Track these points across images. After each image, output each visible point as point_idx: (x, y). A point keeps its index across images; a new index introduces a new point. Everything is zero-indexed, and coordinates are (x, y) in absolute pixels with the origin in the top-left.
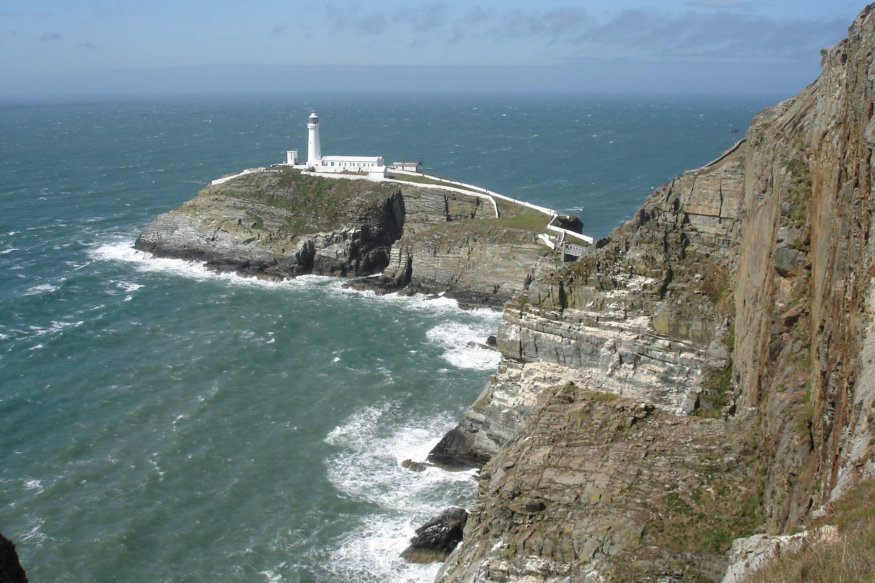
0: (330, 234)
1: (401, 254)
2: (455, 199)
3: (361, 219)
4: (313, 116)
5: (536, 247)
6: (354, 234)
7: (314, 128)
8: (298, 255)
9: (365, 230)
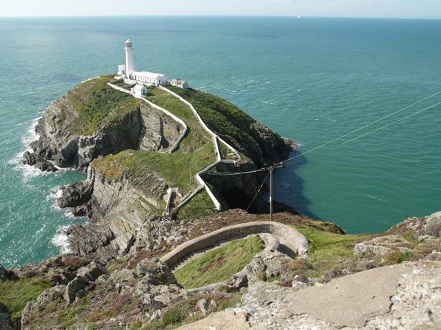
0: (84, 138)
1: (91, 171)
2: (166, 123)
4: (127, 42)
5: (155, 204)
8: (63, 151)
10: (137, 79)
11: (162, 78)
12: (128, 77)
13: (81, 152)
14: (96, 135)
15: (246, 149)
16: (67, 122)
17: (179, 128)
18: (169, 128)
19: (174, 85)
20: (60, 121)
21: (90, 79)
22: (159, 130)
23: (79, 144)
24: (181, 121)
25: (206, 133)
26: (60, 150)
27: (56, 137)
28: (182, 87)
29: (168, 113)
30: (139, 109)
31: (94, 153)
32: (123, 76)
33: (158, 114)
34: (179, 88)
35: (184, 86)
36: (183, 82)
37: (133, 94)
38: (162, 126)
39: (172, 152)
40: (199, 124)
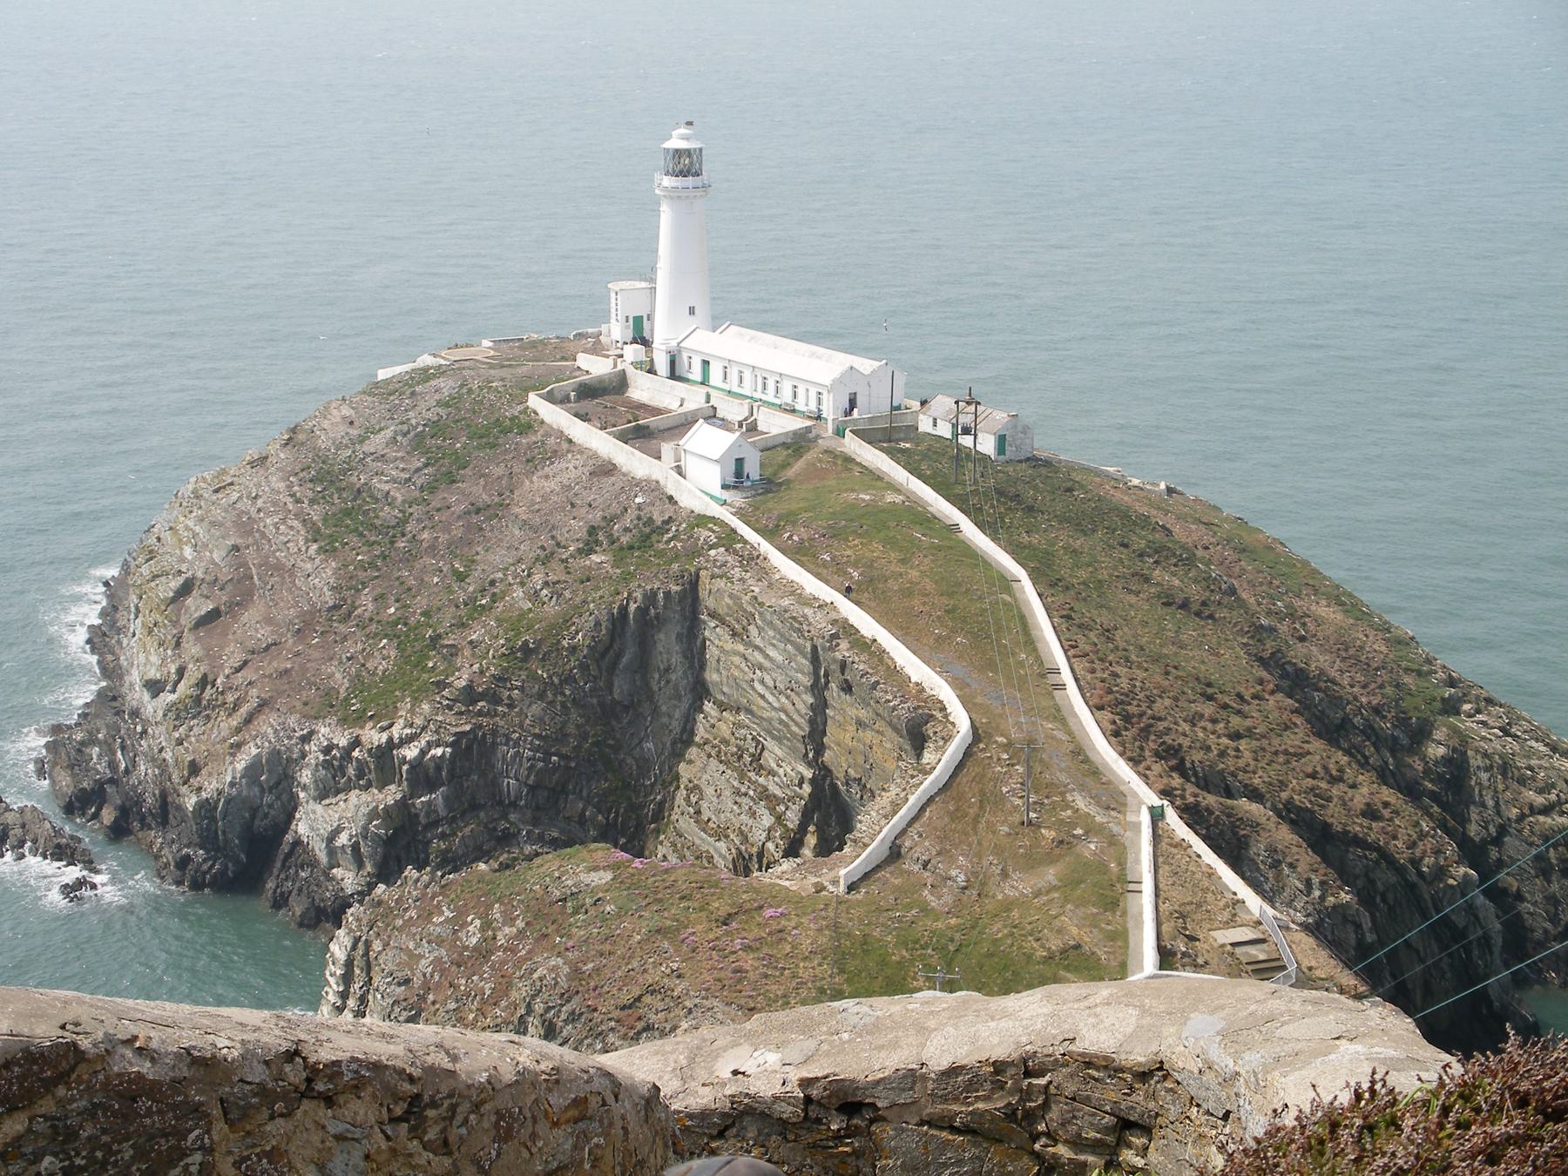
2: (847, 688)
3: (469, 695)
6: (417, 765)
7: (674, 195)
8: (206, 808)
9: (472, 752)
10: (716, 376)
11: (869, 380)
12: (662, 365)
13: (315, 822)
14: (418, 732)
15: (1366, 897)
16: (252, 626)
17: (918, 731)
18: (860, 724)
19: (945, 430)
20: (214, 615)
21: (426, 360)
22: (801, 728)
23: (305, 776)
24: (944, 692)
25: (1090, 770)
26: (190, 802)
27: (179, 713)
28: (987, 445)
29: (866, 625)
30: (694, 583)
31: (388, 842)
32: (633, 352)
33: (797, 625)
34: (963, 457)
35: (1001, 441)
36: (1000, 417)
37: (672, 484)
38: (820, 708)
39: (851, 888)
40: (1060, 716)
